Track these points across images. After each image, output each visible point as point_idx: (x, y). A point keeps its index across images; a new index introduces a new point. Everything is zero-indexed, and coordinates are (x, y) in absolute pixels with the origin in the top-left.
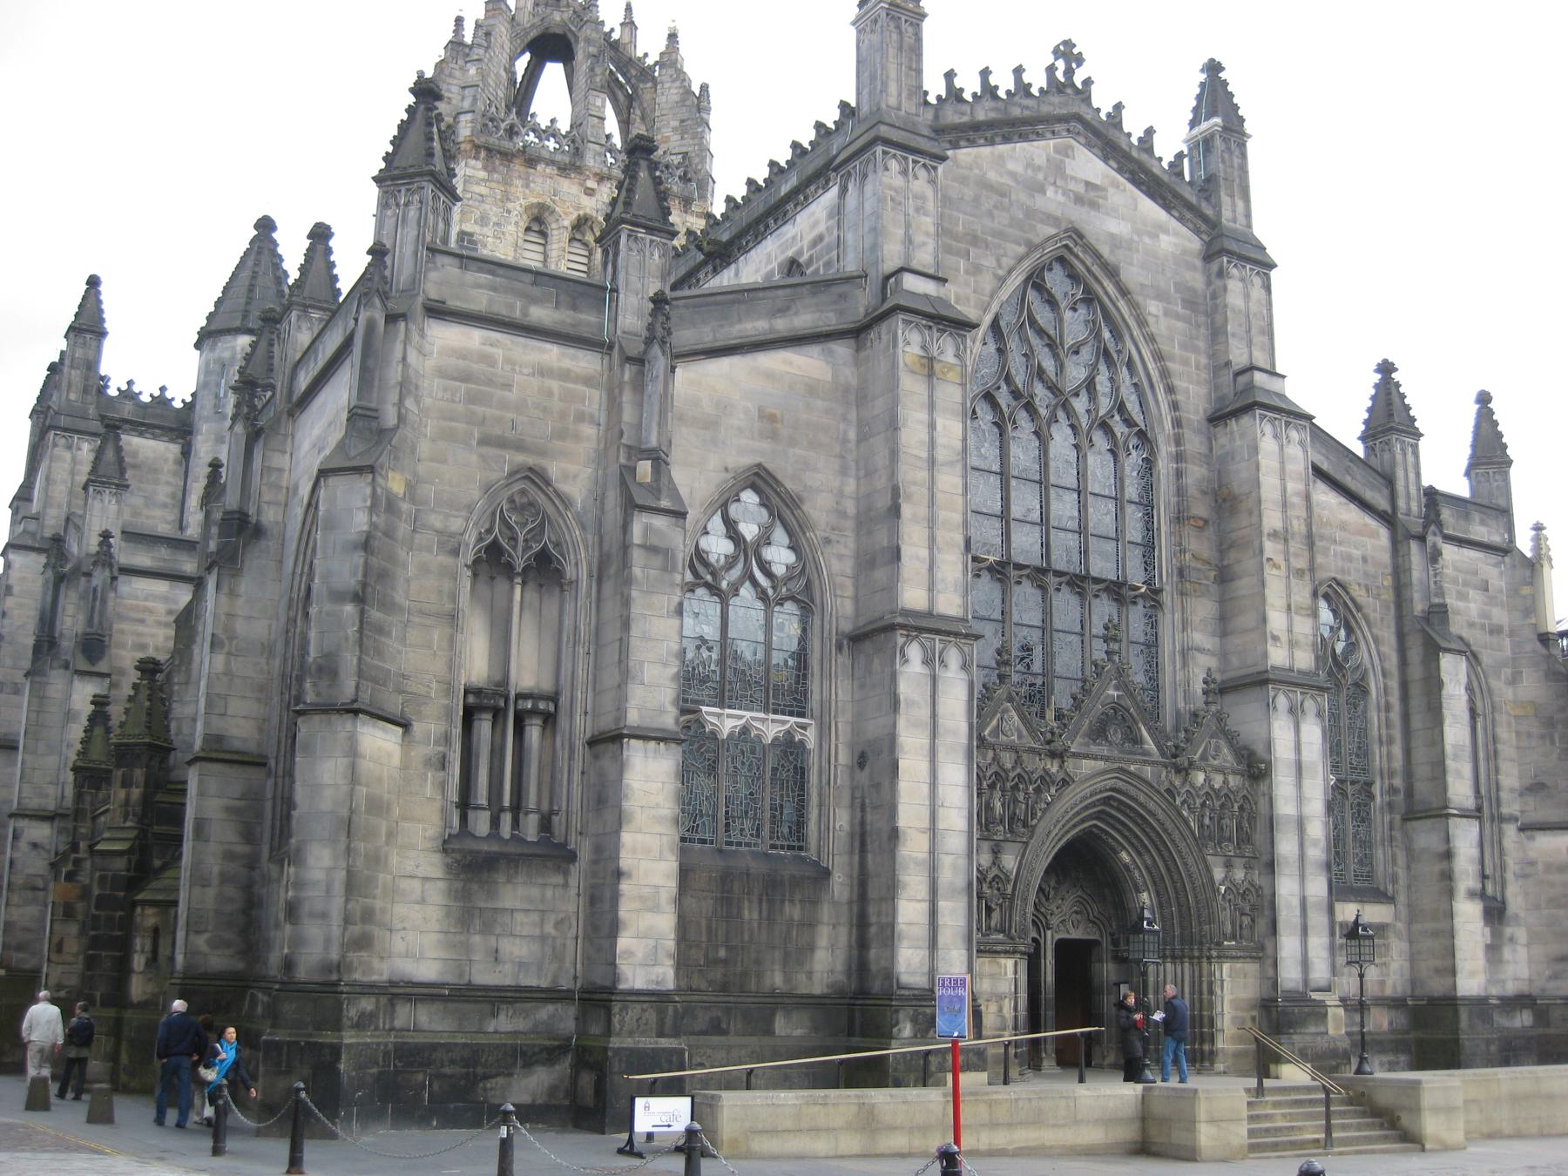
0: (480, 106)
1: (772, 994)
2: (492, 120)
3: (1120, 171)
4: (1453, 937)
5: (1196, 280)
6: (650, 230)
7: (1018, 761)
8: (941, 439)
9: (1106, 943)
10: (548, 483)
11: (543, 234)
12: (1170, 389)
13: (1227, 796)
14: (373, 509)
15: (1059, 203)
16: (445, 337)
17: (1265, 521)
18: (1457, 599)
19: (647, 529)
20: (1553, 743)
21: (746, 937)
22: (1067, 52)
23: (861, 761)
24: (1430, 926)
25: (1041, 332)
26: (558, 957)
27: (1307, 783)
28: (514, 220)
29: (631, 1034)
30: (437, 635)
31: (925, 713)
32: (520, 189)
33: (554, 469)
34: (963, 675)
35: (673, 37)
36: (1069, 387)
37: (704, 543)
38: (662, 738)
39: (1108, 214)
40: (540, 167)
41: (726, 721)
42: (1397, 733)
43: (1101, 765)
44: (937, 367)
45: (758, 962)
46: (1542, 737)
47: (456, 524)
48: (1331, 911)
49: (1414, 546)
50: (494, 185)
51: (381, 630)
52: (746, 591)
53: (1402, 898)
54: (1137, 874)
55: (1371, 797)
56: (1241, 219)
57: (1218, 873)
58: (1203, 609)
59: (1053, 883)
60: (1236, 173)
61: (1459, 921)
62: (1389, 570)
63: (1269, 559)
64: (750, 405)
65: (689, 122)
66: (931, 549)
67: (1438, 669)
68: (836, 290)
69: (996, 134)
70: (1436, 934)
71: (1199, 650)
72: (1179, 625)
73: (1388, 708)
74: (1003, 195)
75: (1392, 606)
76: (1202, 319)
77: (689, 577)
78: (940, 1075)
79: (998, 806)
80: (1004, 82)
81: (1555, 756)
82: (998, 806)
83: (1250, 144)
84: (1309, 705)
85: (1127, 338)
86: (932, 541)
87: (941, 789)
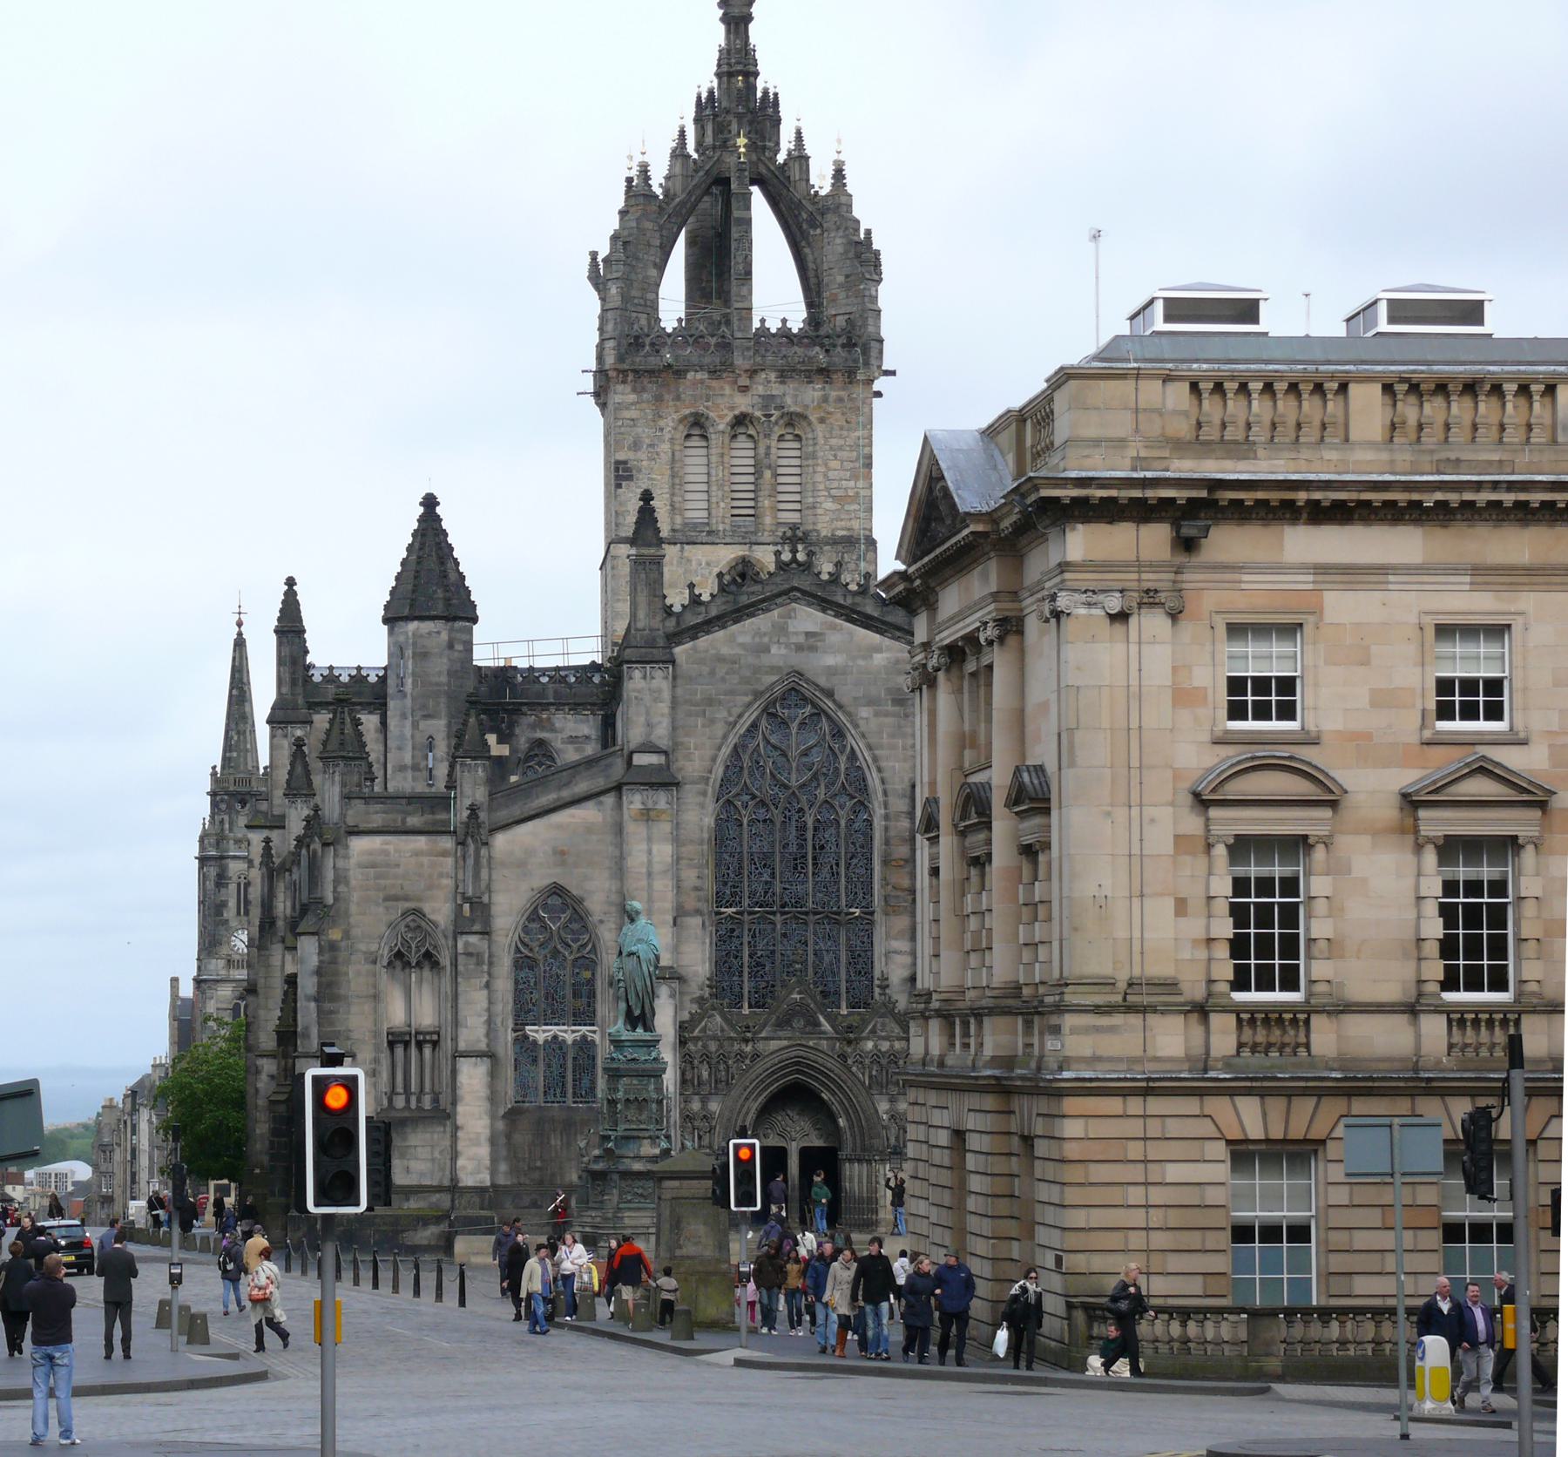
2: (637, 338)
3: (835, 616)
6: (474, 758)
7: (721, 1046)
8: (656, 859)
11: (704, 437)
14: (321, 951)
16: (359, 845)
19: (467, 944)
26: (442, 1169)
28: (667, 436)
29: (465, 1209)
30: (367, 1007)
32: (671, 403)
33: (427, 908)
34: (671, 1001)
35: (839, 175)
38: (479, 1055)
39: (825, 652)
40: (690, 375)
41: (540, 1034)
43: (785, 1043)
45: (561, 1168)
47: (374, 947)
50: (644, 405)
51: (332, 1012)
57: (883, 1106)
65: (852, 278)
68: (603, 763)
71: (895, 952)
79: (705, 1074)
82: (705, 1074)
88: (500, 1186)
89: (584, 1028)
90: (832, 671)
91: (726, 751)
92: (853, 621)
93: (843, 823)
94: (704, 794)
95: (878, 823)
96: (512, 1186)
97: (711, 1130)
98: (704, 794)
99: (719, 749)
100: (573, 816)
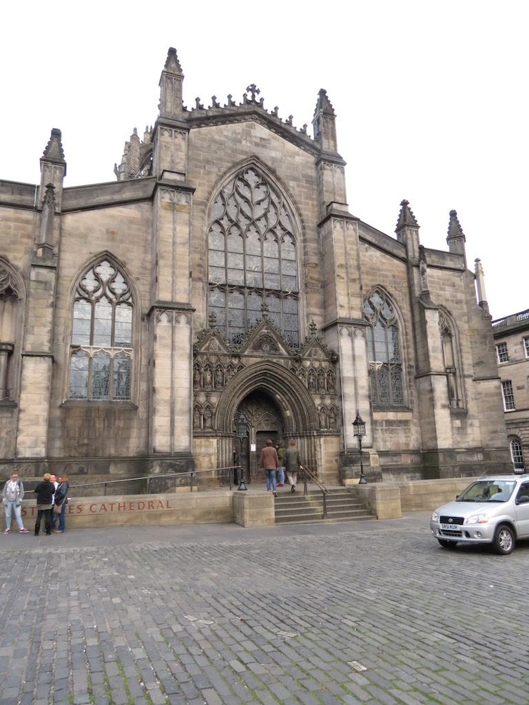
0: (127, 170)
1: (110, 457)
3: (276, 133)
4: (435, 424)
5: (312, 173)
7: (219, 360)
8: (179, 235)
9: (280, 432)
10: (8, 262)
12: (300, 215)
13: (322, 370)
15: (248, 146)
17: (336, 260)
18: (440, 290)
19: (38, 274)
20: (486, 345)
21: (97, 434)
22: (253, 89)
23: (149, 363)
24: (427, 420)
25: (242, 197)
27: (358, 363)
31: (169, 341)
33: (10, 256)
34: (188, 326)
36: (256, 217)
37: (84, 282)
42: (411, 344)
44: (177, 207)
45: (102, 444)
46: (481, 343)
48: (371, 415)
49: (415, 270)
52: (104, 300)
53: (416, 409)
54: (284, 403)
55: (401, 370)
56: (333, 148)
57: (317, 402)
58: (316, 298)
59: (254, 409)
60: (330, 131)
61: (436, 418)
62: (406, 280)
63: (338, 276)
64: (102, 229)
66: (173, 277)
67: (425, 317)
68: (142, 183)
69: (218, 121)
70: (429, 423)
72: (305, 305)
73: (407, 334)
74: (222, 144)
75: (408, 294)
76: (315, 187)
77: (77, 296)
78: (174, 488)
79: (209, 378)
80: (223, 102)
81: (487, 350)
82: (209, 378)
83: (337, 120)
84: (359, 332)
85: (282, 197)
86: (173, 273)
87: (176, 372)
88: (54, 458)
89: (123, 349)
90: (274, 160)
91: (216, 192)
92: (284, 137)
93: (280, 242)
94: (204, 212)
95: (299, 244)
96: (65, 458)
97: (213, 415)
98: (204, 212)
99: (213, 189)
100: (122, 212)
